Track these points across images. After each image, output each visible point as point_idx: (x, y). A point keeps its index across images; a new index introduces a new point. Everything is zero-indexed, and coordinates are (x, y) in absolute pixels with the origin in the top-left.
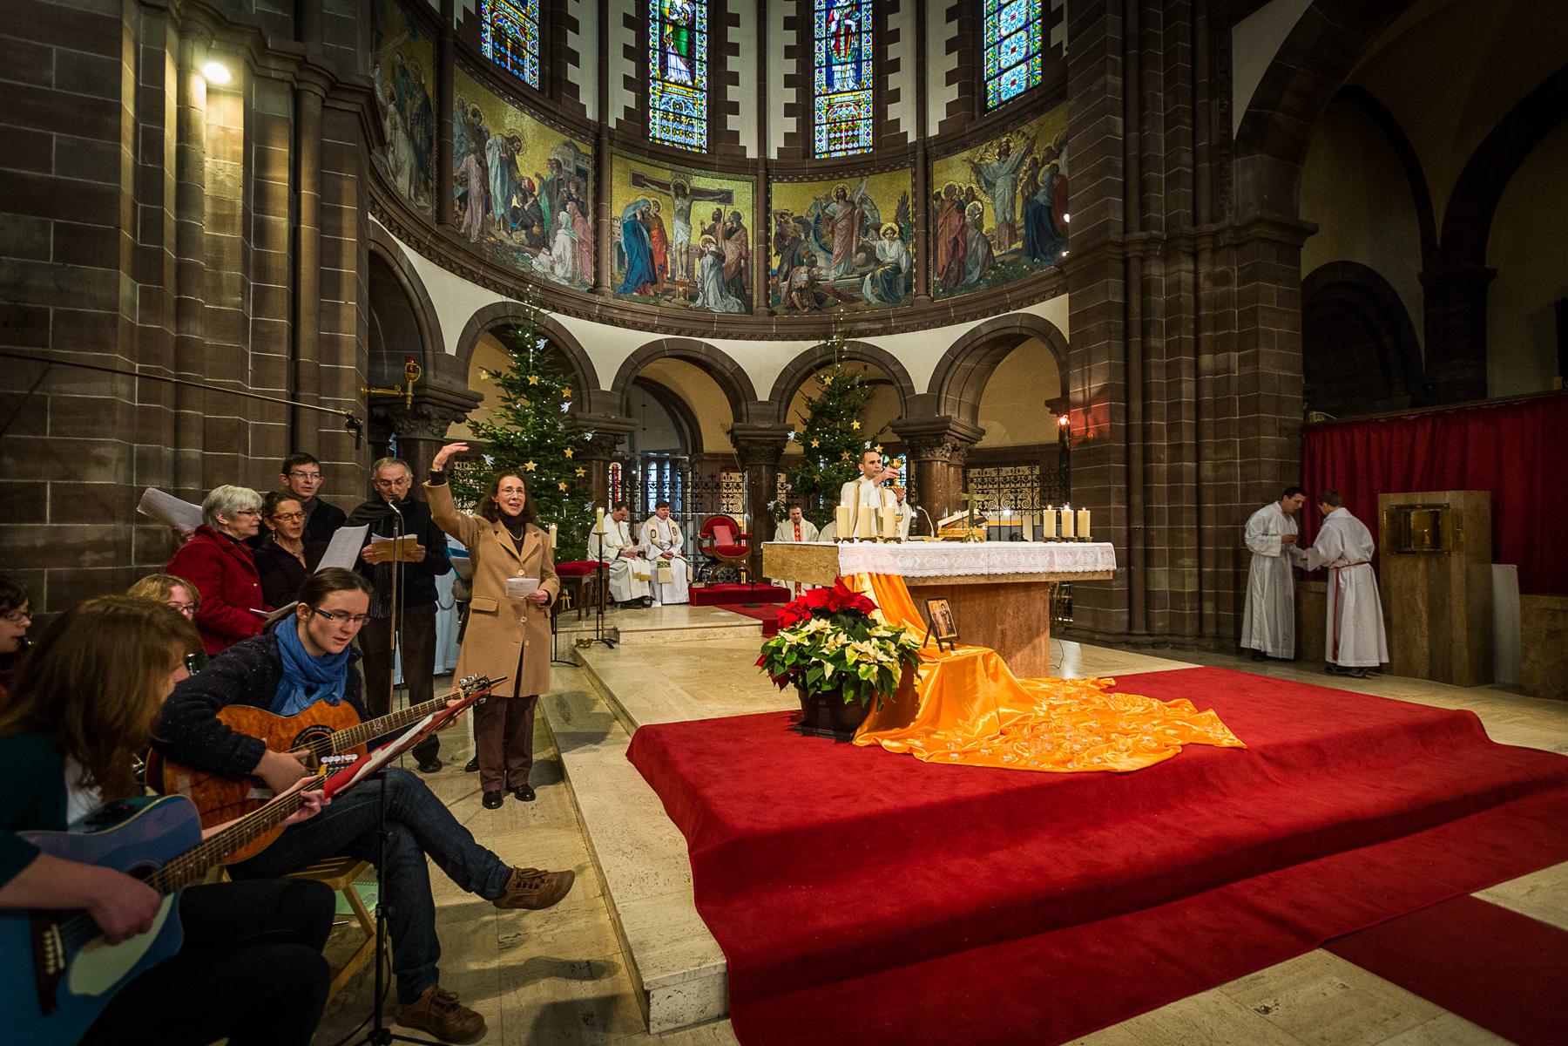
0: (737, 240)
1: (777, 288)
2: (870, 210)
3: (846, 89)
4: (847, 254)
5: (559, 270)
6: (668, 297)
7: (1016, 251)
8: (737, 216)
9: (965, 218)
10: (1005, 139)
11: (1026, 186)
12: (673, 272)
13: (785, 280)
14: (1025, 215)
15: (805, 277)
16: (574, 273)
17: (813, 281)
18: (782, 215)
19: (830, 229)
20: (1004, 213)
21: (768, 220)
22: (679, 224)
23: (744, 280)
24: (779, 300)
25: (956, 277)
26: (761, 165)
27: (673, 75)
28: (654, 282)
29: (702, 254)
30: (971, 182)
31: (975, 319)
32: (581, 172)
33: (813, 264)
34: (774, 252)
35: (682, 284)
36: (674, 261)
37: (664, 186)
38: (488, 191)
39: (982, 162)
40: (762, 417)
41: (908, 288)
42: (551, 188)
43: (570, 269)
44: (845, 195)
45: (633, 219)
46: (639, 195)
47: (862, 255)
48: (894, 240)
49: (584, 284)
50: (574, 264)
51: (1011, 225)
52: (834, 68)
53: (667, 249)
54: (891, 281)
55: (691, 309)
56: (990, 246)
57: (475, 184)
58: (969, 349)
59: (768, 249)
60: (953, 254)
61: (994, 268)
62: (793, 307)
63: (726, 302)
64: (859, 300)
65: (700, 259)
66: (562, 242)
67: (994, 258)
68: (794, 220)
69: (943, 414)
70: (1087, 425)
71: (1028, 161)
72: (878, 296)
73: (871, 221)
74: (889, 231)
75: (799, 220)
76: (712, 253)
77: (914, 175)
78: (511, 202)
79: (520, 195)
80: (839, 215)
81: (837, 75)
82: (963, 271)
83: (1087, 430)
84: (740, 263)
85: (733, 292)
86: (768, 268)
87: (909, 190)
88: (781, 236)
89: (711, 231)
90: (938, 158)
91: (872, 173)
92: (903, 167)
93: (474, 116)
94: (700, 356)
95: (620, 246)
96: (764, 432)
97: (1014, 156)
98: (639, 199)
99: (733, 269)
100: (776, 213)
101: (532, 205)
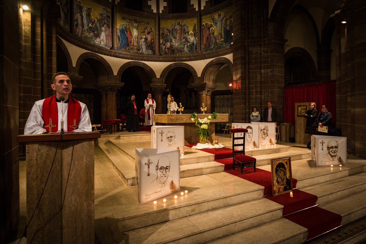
0: (151, 35)
1: (162, 48)
2: (186, 28)
4: (180, 39)
5: (102, 43)
6: (132, 50)
7: (222, 41)
9: (210, 31)
10: (219, 12)
11: (224, 25)
12: (134, 43)
13: (164, 46)
14: (224, 32)
15: (169, 45)
16: (106, 44)
17: (171, 46)
19: (176, 32)
20: (219, 31)
23: (153, 45)
24: (162, 51)
25: (208, 47)
30: (211, 22)
31: (212, 58)
32: (108, 16)
33: (171, 41)
35: (136, 46)
36: (134, 40)
38: (83, 23)
39: (214, 18)
41: (196, 49)
42: (100, 21)
43: (105, 43)
44: (180, 23)
45: (122, 29)
47: (184, 40)
48: (192, 36)
49: (109, 47)
50: (106, 41)
51: (221, 34)
53: (132, 37)
54: (192, 47)
55: (138, 53)
56: (216, 39)
58: (211, 65)
60: (207, 41)
61: (217, 45)
62: (166, 53)
64: (184, 51)
66: (103, 35)
67: (217, 42)
68: (166, 29)
69: (204, 82)
70: (236, 86)
71: (225, 18)
73: (186, 31)
74: (191, 34)
75: (167, 30)
76: (144, 38)
77: (197, 19)
78: (89, 25)
79: (92, 23)
82: (210, 45)
83: (237, 87)
84: (152, 41)
85: (150, 49)
87: (196, 23)
90: (204, 15)
91: (187, 18)
92: (195, 17)
93: (79, 3)
94: (141, 66)
96: (158, 86)
97: (222, 17)
98: (124, 23)
99: (150, 42)
101: (95, 26)
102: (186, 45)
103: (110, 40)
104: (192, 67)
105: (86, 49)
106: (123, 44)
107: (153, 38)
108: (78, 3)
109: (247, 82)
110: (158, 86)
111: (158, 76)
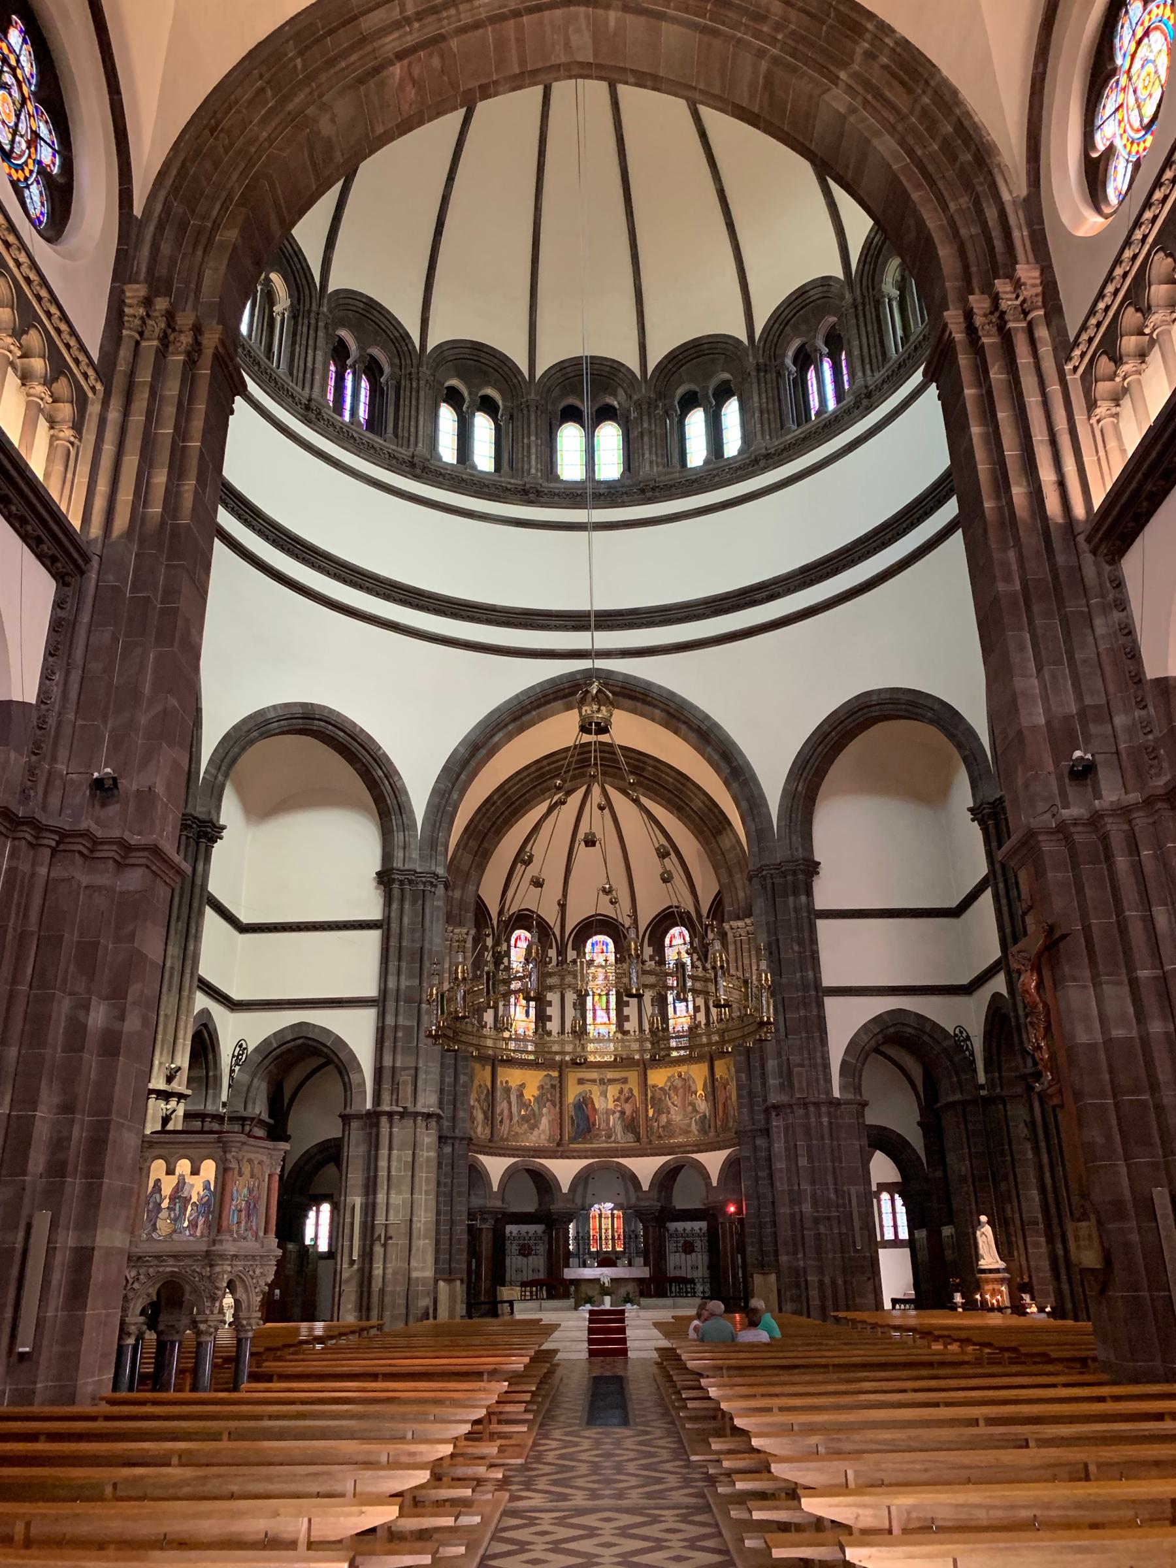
4: (684, 1107)
5: (543, 1137)
8: (631, 1090)
17: (669, 1122)
22: (602, 1099)
27: (599, 1020)
28: (589, 1131)
29: (614, 1113)
33: (669, 1113)
42: (537, 1099)
46: (581, 1088)
57: (506, 1113)
62: (660, 1137)
66: (544, 1123)
75: (661, 1089)
89: (618, 1100)
103: (557, 1128)
109: (756, 1202)
111: (645, 1187)
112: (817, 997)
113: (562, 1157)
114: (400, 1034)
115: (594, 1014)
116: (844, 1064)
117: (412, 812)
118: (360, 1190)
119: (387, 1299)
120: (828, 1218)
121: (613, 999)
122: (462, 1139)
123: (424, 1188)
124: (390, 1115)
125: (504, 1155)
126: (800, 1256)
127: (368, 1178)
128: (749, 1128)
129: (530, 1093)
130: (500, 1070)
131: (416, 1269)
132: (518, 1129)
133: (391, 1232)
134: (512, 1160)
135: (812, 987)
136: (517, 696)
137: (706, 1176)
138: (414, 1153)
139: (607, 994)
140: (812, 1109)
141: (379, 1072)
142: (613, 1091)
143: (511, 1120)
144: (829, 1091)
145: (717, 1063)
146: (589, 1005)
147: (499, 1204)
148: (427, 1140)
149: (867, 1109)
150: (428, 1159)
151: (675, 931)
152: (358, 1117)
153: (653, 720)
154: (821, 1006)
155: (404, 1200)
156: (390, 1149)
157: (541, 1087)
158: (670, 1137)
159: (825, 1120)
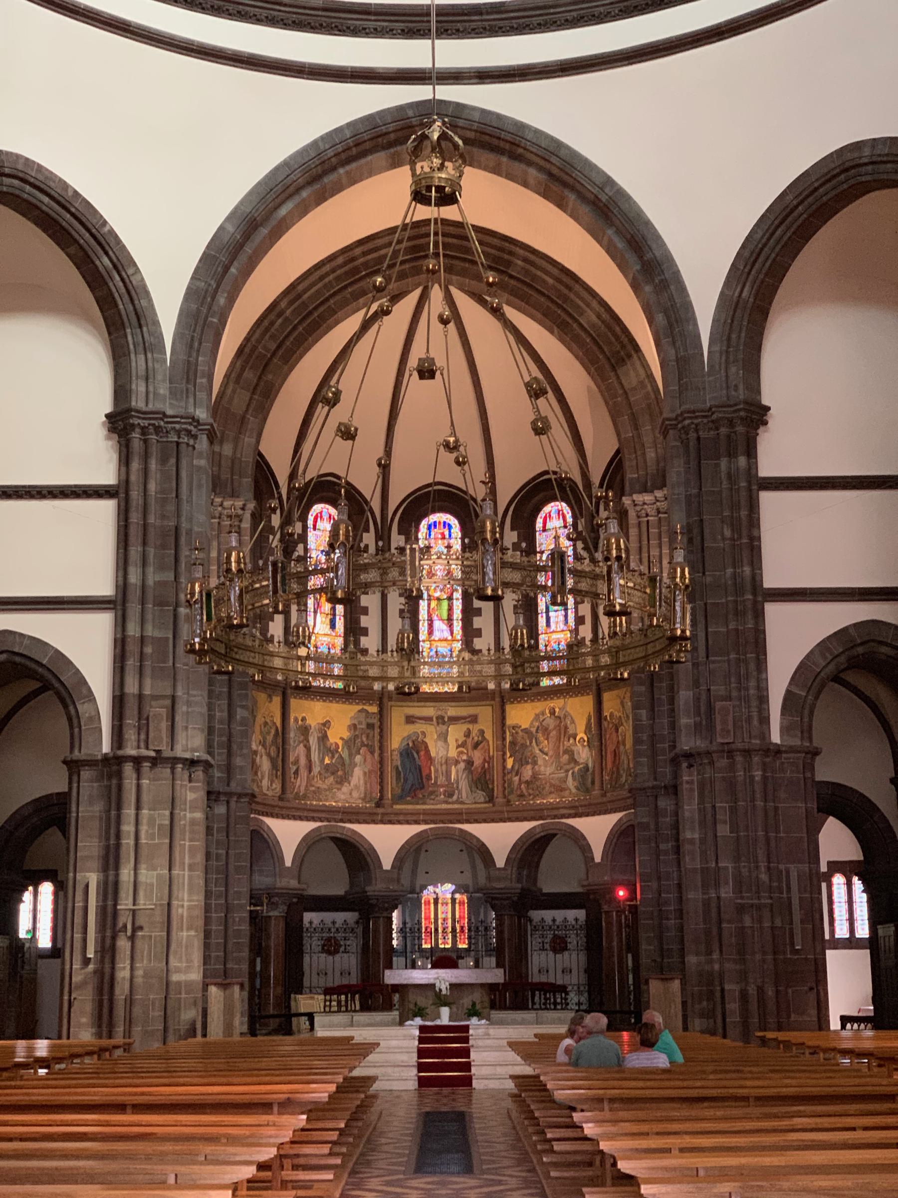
1: (511, 783)
3: (559, 629)
4: (558, 756)
6: (433, 797)
8: (482, 732)
12: (436, 778)
13: (517, 775)
15: (530, 773)
16: (365, 793)
17: (535, 776)
18: (513, 728)
21: (504, 732)
23: (488, 777)
26: (497, 695)
27: (437, 635)
28: (422, 787)
29: (457, 762)
33: (535, 763)
34: (508, 755)
35: (442, 786)
36: (436, 771)
37: (428, 719)
40: (499, 879)
42: (348, 743)
43: (363, 792)
44: (555, 712)
46: (411, 729)
47: (566, 757)
50: (366, 788)
52: (551, 614)
57: (303, 761)
59: (504, 754)
62: (522, 796)
63: (474, 795)
65: (456, 765)
66: (358, 775)
72: (577, 788)
75: (526, 731)
76: (464, 761)
80: (551, 727)
81: (552, 620)
82: (619, 776)
86: (504, 767)
88: (513, 743)
89: (463, 745)
90: (606, 691)
91: (571, 696)
92: (588, 694)
95: (397, 768)
99: (479, 770)
100: (509, 727)
102: (570, 772)
103: (375, 780)
104: (582, 835)
105: (313, 819)
106: (408, 787)
107: (487, 758)
108: (300, 722)
109: (654, 885)
110: (501, 889)
111: (500, 862)
112: (755, 602)
113: (382, 822)
114: (148, 650)
115: (431, 626)
116: (789, 696)
117: (157, 323)
118: (95, 864)
119: (137, 1010)
120: (759, 907)
121: (458, 606)
122: (240, 796)
123: (187, 861)
124: (137, 761)
125: (301, 819)
126: (716, 956)
127: (107, 848)
128: (650, 784)
129: (338, 734)
130: (294, 702)
131: (178, 970)
132: (320, 784)
133: (140, 921)
134: (313, 825)
135: (748, 586)
136: (315, 143)
137: (584, 847)
138: (172, 814)
139: (450, 598)
140: (739, 758)
141: (119, 701)
142: (455, 733)
143: (310, 771)
144: (765, 734)
145: (606, 696)
146: (423, 614)
147: (294, 883)
148: (190, 796)
149: (818, 758)
150: (193, 822)
151: (551, 508)
152: (90, 763)
153: (525, 184)
154: (759, 615)
155: (159, 877)
156: (138, 808)
157: (354, 727)
158: (540, 795)
159: (758, 774)
